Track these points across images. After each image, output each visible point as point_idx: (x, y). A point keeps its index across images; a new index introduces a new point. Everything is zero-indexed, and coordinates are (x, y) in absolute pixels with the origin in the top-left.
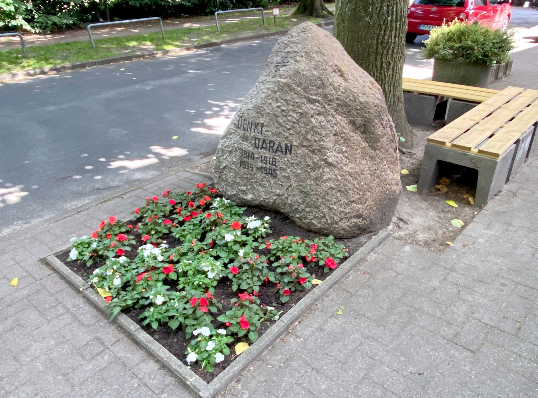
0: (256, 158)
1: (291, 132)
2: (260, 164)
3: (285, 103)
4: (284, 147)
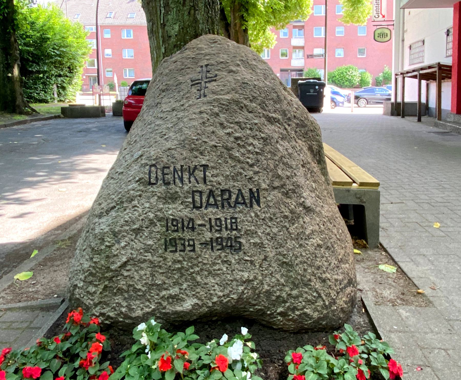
0: (199, 225)
1: (256, 169)
2: (208, 235)
3: (237, 127)
4: (247, 195)
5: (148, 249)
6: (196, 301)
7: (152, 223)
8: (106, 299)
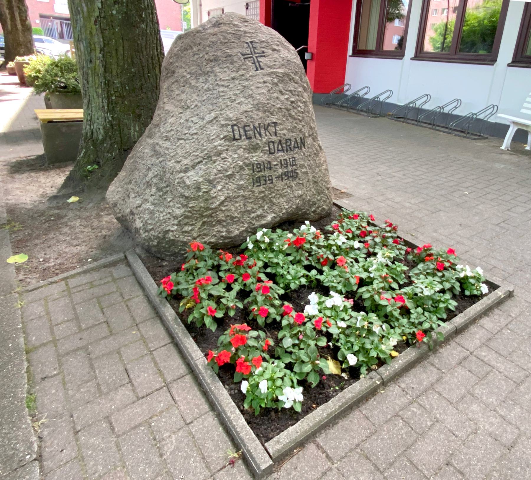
0: (275, 165)
2: (280, 171)
5: (240, 188)
6: (273, 215)
7: (242, 168)
8: (205, 232)
